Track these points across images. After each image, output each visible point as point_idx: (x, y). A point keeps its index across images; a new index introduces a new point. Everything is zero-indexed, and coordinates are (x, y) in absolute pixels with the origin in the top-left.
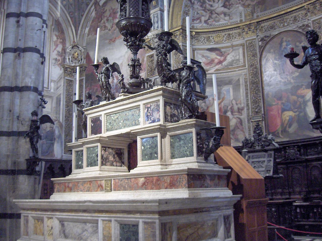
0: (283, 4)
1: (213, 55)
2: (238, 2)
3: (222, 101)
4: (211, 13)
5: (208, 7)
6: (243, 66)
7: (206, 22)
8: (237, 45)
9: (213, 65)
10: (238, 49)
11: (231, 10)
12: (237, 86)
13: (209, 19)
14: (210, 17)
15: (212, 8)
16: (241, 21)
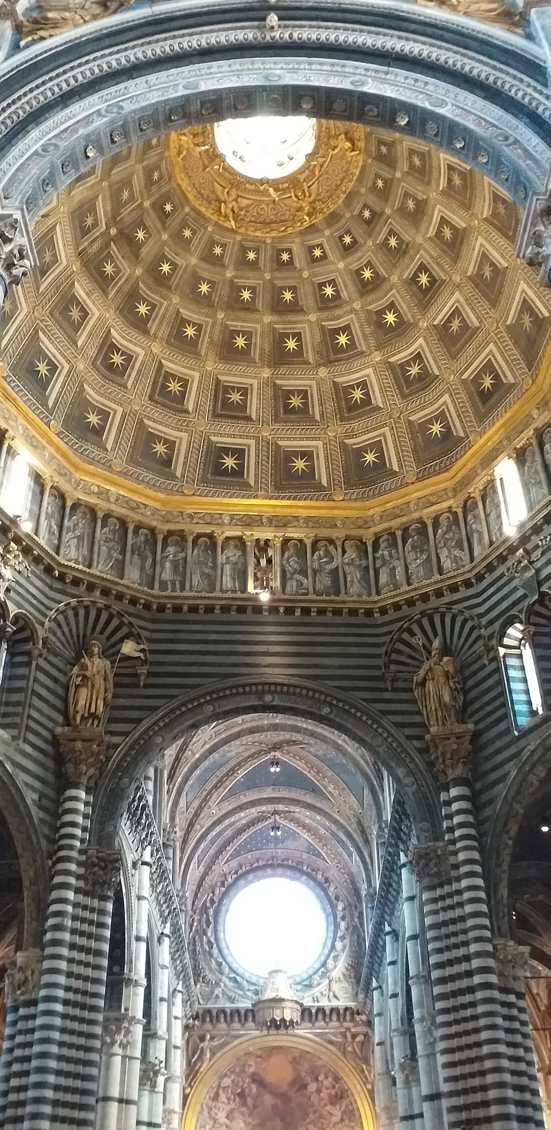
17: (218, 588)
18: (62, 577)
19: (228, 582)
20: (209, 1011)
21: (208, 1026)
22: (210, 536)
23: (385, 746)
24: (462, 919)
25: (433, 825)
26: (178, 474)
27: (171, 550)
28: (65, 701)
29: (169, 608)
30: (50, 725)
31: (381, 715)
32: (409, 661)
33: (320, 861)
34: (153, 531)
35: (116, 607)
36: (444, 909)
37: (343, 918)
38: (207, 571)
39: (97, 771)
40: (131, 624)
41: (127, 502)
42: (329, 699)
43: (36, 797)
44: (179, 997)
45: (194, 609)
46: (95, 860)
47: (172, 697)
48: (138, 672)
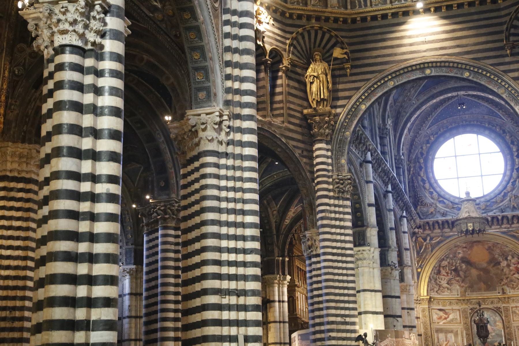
0: (485, 291)
1: (441, 313)
2: (457, 283)
3: (448, 343)
4: (440, 286)
5: (438, 282)
6: (459, 323)
7: (437, 292)
8: (455, 310)
9: (441, 320)
10: (456, 312)
11: (452, 287)
12: (456, 335)
13: (438, 290)
14: (439, 289)
15: (440, 284)
16: (458, 295)
18: (291, 15)
21: (428, 232)
23: (507, 93)
28: (305, 92)
29: (358, 21)
30: (299, 109)
31: (503, 74)
35: (326, 28)
39: (330, 131)
40: (336, 36)
42: (468, 67)
43: (300, 152)
45: (374, 18)
46: (337, 180)
47: (368, 80)
48: (345, 66)
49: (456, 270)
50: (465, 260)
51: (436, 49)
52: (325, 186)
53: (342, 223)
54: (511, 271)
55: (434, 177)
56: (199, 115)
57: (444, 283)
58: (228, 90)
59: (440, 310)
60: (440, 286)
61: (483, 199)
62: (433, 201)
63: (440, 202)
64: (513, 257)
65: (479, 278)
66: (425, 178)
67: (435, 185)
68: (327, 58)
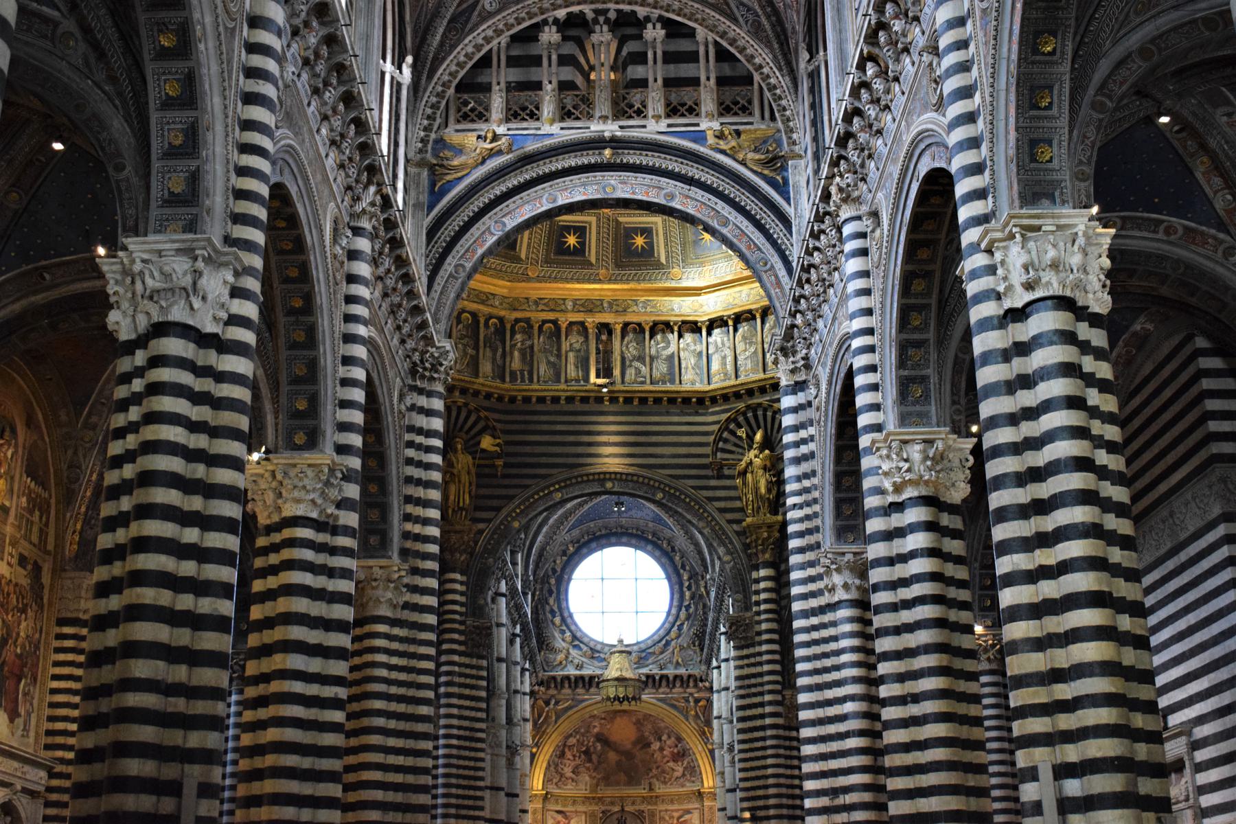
1: (559, 817)
17: (563, 380)
19: (572, 371)
20: (554, 678)
21: (552, 692)
22: (555, 322)
24: (761, 675)
25: (745, 597)
26: (523, 256)
27: (518, 337)
32: (734, 449)
33: (666, 531)
34: (501, 319)
35: (472, 405)
36: (748, 666)
37: (689, 588)
38: (552, 359)
40: (487, 418)
41: (477, 296)
44: (527, 673)
45: (541, 400)
47: (527, 487)
49: (587, 753)
50: (601, 738)
51: (622, 456)
52: (456, 636)
53: (474, 693)
54: (664, 757)
55: (568, 608)
56: (371, 567)
57: (568, 771)
58: (406, 535)
59: (559, 812)
60: (562, 775)
61: (635, 648)
62: (564, 644)
63: (575, 647)
64: (669, 737)
65: (619, 763)
66: (555, 608)
67: (569, 621)
68: (472, 447)
